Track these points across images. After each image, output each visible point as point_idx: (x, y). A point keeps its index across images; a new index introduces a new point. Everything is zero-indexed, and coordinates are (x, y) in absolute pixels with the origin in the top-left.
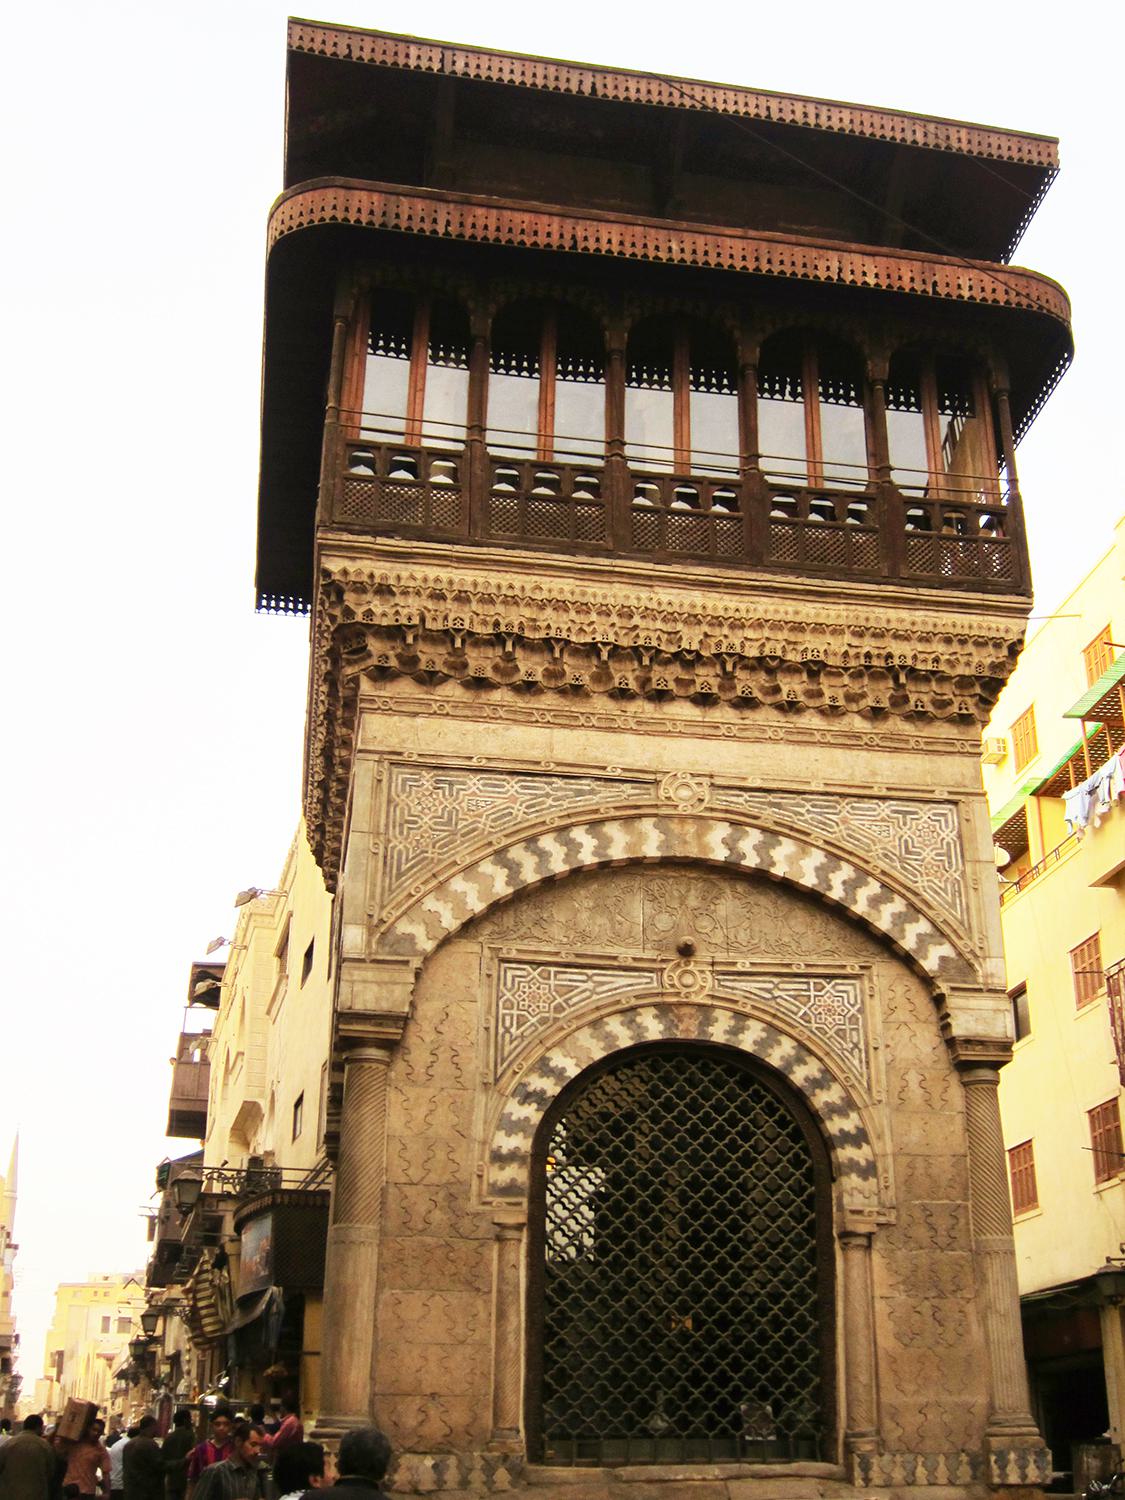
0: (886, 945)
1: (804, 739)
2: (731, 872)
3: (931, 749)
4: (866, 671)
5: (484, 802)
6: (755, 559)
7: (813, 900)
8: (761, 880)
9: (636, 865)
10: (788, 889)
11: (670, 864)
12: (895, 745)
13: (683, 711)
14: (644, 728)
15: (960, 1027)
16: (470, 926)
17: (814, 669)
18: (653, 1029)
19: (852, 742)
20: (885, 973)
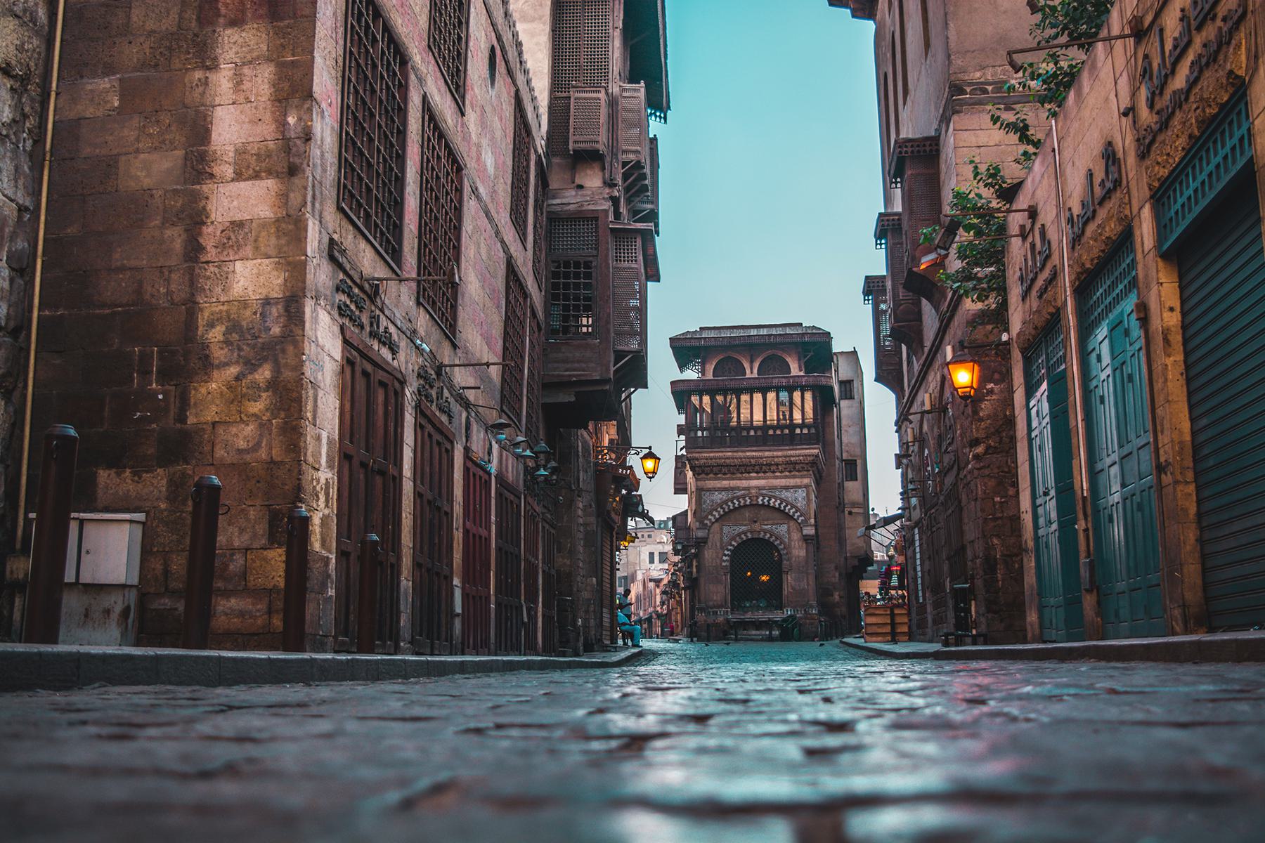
0: (792, 517)
1: (777, 478)
2: (763, 505)
3: (802, 477)
4: (787, 463)
5: (718, 497)
6: (765, 445)
7: (778, 509)
8: (768, 506)
9: (745, 506)
10: (773, 507)
11: (751, 505)
12: (794, 477)
13: (753, 475)
14: (746, 479)
15: (805, 532)
16: (717, 520)
17: (777, 465)
18: (749, 536)
19: (786, 477)
20: (792, 523)
